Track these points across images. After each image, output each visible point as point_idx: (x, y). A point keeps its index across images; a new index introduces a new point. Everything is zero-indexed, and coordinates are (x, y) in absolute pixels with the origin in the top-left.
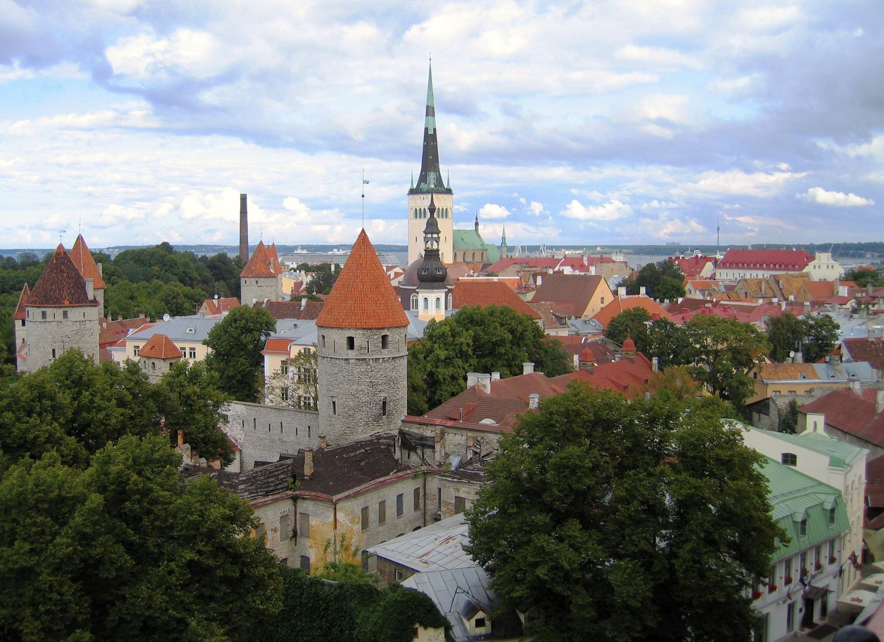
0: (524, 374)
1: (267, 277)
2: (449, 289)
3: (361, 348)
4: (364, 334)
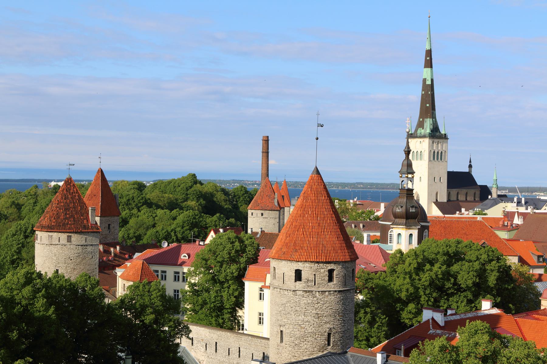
0: (483, 309)
1: (272, 210)
2: (422, 226)
3: (308, 280)
4: (311, 268)
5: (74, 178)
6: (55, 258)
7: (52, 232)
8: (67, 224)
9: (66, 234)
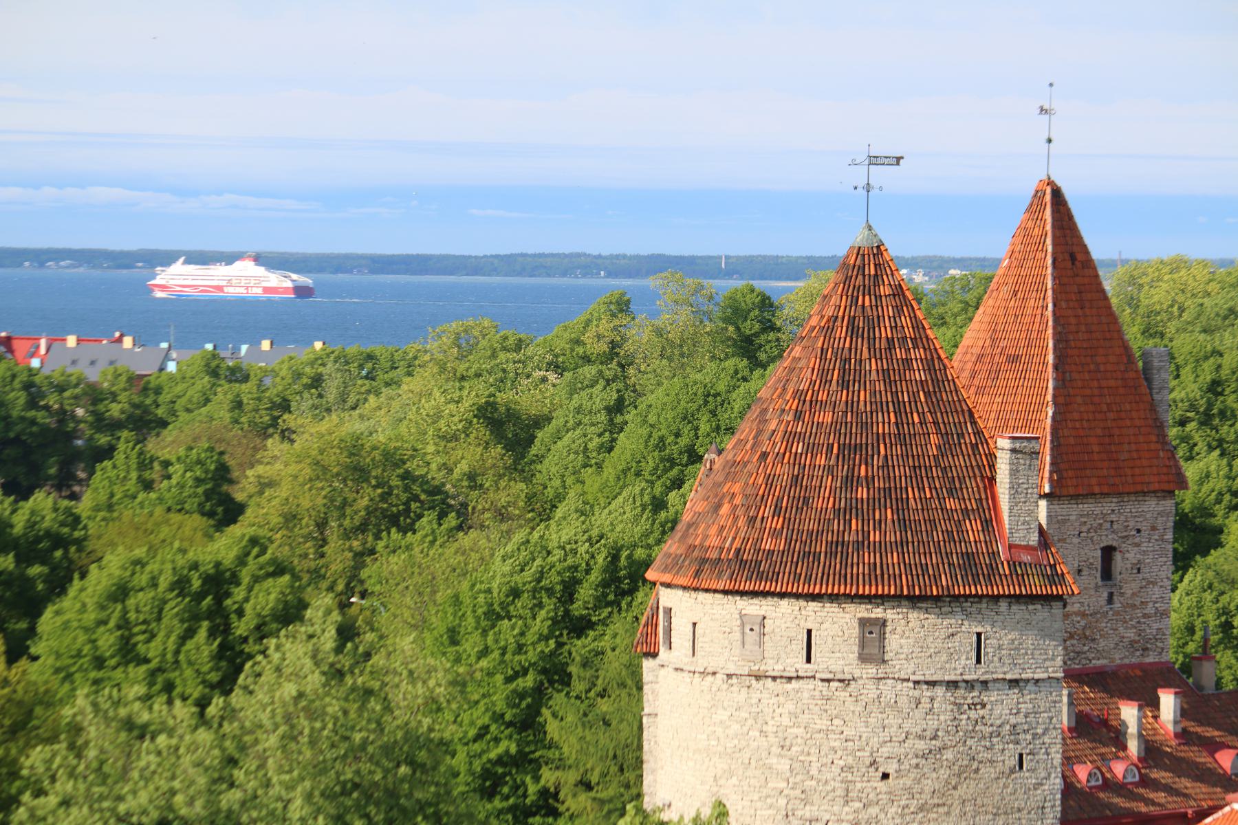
5: (895, 248)
6: (784, 765)
7: (765, 594)
8: (859, 545)
9: (850, 607)
